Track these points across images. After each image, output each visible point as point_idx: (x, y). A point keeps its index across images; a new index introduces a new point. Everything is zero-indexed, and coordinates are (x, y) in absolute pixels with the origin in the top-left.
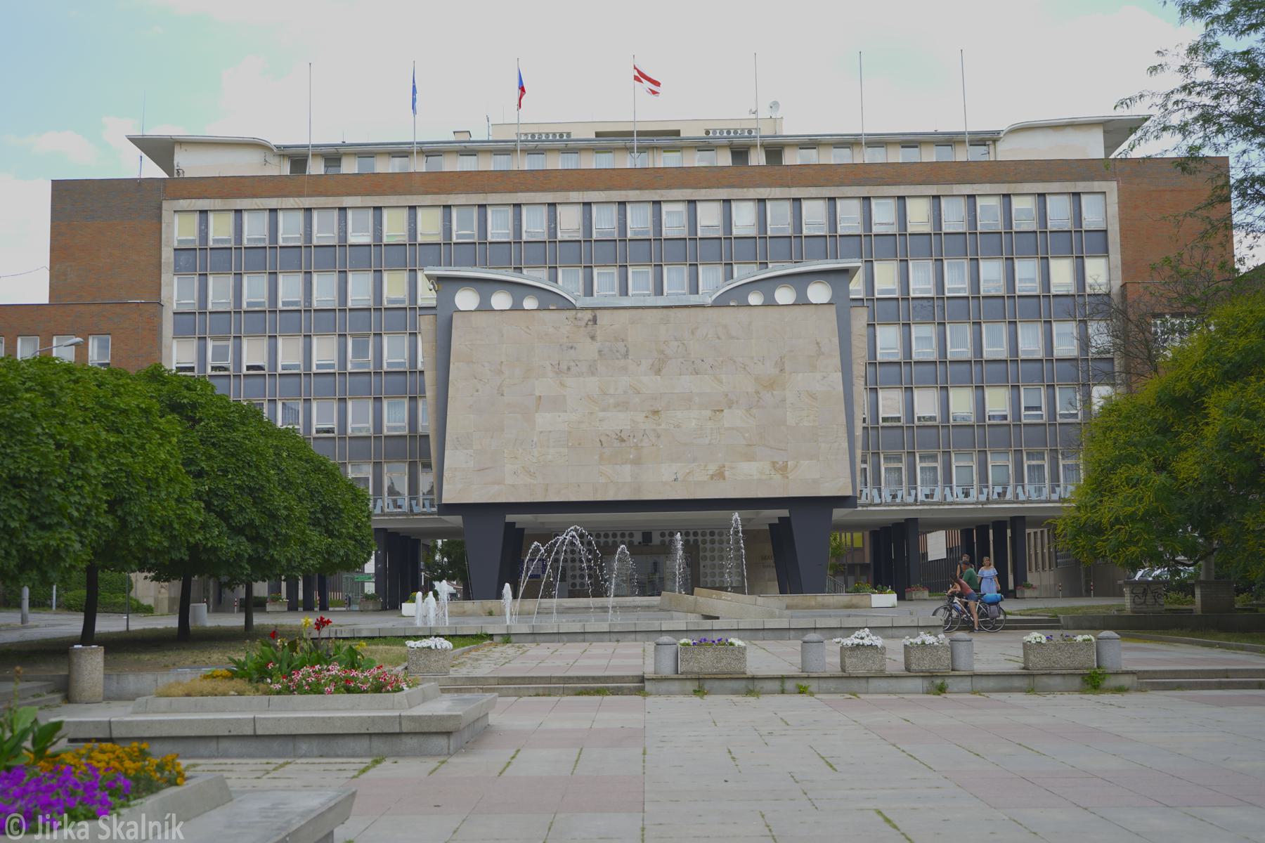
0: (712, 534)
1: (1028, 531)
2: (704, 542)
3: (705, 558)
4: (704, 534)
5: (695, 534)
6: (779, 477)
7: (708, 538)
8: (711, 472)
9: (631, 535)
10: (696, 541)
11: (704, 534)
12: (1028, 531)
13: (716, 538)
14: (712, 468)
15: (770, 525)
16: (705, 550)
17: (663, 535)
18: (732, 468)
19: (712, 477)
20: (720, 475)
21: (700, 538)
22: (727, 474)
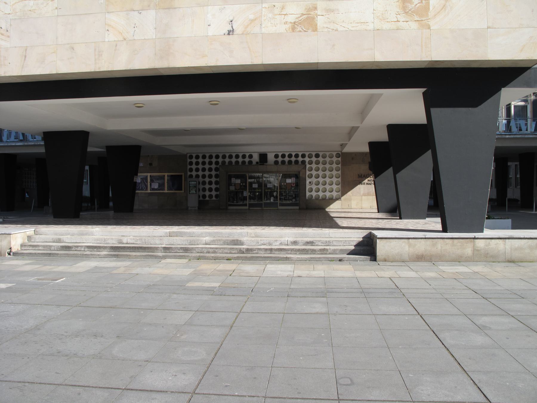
0: (317, 156)
1: (509, 164)
2: (311, 163)
3: (311, 176)
4: (310, 156)
5: (303, 156)
6: (414, 25)
7: (314, 159)
8: (291, 19)
9: (251, 156)
10: (303, 162)
11: (310, 156)
12: (509, 164)
13: (321, 159)
14: (294, 11)
15: (372, 145)
16: (311, 169)
17: (276, 156)
18: (329, 11)
19: (294, 26)
20: (307, 23)
21: (307, 159)
22: (320, 21)
